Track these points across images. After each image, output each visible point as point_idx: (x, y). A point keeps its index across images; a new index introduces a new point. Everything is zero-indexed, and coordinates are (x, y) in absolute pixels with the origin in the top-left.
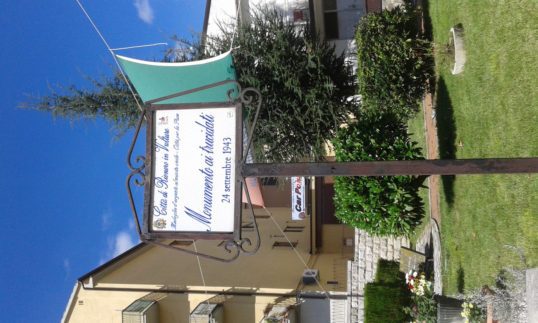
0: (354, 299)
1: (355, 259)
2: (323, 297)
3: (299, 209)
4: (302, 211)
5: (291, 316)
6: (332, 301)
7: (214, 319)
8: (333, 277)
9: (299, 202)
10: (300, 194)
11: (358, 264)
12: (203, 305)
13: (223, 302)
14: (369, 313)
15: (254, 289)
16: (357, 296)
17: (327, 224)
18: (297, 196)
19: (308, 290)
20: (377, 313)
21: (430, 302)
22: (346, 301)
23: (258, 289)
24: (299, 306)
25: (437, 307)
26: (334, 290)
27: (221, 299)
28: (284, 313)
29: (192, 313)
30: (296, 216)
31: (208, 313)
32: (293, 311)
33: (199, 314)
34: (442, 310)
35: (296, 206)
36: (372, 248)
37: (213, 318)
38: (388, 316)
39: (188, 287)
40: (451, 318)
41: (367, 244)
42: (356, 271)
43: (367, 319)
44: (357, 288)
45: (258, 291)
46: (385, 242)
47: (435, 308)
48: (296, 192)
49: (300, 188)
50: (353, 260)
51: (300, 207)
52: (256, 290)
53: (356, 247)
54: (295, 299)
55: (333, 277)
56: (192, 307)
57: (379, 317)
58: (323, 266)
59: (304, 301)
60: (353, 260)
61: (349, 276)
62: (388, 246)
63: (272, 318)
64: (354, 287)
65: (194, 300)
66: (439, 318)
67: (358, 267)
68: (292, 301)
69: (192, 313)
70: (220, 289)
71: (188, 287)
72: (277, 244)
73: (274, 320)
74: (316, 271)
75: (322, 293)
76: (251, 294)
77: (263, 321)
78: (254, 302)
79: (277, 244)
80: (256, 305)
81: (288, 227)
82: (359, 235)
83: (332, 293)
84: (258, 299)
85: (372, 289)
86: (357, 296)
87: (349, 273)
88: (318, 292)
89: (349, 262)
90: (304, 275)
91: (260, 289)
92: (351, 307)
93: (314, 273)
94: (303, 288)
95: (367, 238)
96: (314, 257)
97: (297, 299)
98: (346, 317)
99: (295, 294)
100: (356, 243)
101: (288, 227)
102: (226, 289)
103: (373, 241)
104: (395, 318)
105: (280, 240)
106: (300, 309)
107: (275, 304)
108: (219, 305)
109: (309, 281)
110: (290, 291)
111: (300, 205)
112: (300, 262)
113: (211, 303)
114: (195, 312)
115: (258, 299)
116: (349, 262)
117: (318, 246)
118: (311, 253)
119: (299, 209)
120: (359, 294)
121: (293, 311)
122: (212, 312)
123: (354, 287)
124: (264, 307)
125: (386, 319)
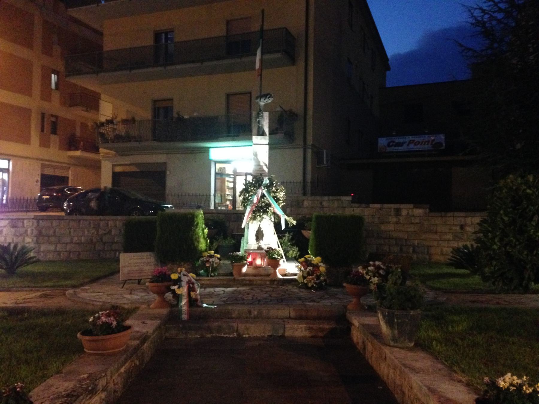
1: (353, 205)
3: (391, 144)
10: (408, 145)
18: (405, 142)
35: (394, 142)
50: (353, 202)
60: (353, 202)
111: (395, 146)
116: (349, 198)
119: (391, 144)
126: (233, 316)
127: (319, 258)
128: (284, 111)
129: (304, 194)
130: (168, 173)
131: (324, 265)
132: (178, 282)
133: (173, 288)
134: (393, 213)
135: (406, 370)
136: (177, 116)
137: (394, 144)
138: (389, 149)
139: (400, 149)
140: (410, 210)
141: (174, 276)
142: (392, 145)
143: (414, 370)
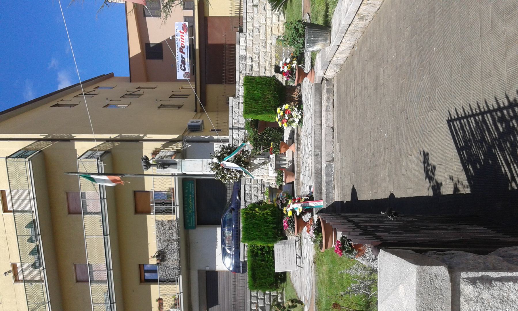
0: (236, 132)
4: (187, 71)
6: (215, 144)
7: (102, 163)
9: (183, 62)
10: (184, 53)
11: (239, 99)
13: (111, 149)
14: (247, 100)
15: (141, 135)
16: (238, 128)
17: (211, 83)
18: (182, 55)
19: (194, 136)
20: (254, 100)
23: (145, 135)
25: (305, 29)
27: (108, 146)
29: (79, 158)
33: (87, 158)
35: (181, 65)
37: (101, 161)
38: (264, 102)
39: (73, 135)
44: (238, 121)
45: (145, 138)
48: (180, 51)
49: (184, 47)
50: (234, 96)
52: (144, 136)
54: (181, 143)
56: (79, 154)
59: (189, 146)
60: (234, 96)
61: (231, 111)
65: (81, 147)
66: (307, 38)
67: (239, 103)
69: (79, 158)
71: (73, 135)
74: (201, 120)
75: (206, 138)
76: (139, 141)
78: (142, 148)
80: (143, 150)
82: (240, 72)
83: (215, 137)
85: (251, 79)
86: (238, 128)
87: (230, 108)
89: (231, 98)
90: (190, 123)
91: (147, 135)
93: (199, 122)
96: (199, 114)
97: (183, 144)
99: (181, 139)
101: (173, 95)
102: (113, 136)
104: (270, 103)
105: (164, 103)
108: (106, 152)
109: (194, 128)
110: (176, 136)
111: (185, 64)
113: (99, 150)
114: (83, 157)
115: (145, 144)
117: (203, 104)
118: (196, 111)
122: (100, 156)
127: (278, 110)
130: (207, 269)
132: (294, 211)
133: (298, 214)
134: (243, 62)
136: (155, 259)
137: (183, 65)
138: (188, 70)
139: (187, 60)
140: (241, 47)
141: (290, 214)
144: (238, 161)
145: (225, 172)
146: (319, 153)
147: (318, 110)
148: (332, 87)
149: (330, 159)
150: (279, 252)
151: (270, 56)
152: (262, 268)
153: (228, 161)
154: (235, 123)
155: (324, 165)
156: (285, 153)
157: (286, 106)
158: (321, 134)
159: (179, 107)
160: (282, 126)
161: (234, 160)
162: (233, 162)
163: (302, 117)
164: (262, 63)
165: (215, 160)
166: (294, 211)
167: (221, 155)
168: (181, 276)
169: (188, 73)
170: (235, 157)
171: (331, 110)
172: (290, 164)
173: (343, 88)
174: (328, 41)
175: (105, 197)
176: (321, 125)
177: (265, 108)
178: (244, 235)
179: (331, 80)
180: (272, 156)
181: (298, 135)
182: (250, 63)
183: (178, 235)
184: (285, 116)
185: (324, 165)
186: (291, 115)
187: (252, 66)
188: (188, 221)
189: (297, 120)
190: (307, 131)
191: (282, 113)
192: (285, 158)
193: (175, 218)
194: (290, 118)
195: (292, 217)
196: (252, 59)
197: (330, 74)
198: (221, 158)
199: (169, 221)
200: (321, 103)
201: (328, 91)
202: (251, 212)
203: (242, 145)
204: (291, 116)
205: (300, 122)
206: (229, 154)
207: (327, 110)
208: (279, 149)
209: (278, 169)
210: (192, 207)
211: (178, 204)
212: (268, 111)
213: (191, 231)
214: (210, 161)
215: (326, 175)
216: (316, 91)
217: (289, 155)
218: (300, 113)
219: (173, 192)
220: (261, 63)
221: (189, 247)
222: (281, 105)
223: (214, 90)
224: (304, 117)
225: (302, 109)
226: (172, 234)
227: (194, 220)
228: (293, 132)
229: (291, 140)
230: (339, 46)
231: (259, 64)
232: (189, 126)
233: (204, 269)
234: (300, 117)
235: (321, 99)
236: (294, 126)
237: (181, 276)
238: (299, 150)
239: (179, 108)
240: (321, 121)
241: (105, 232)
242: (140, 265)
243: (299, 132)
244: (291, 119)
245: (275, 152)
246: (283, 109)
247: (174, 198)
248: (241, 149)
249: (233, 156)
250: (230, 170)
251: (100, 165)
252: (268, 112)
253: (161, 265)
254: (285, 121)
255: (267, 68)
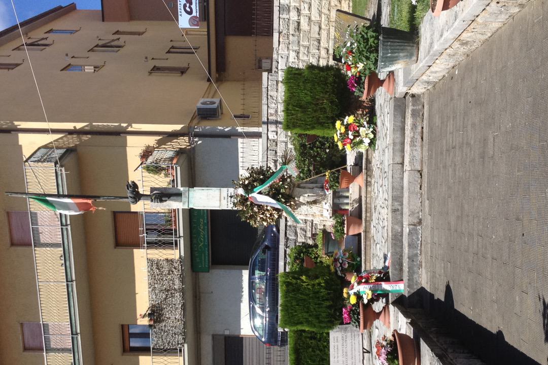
0: (272, 128)
1: (274, 69)
2: (227, 136)
3: (188, 9)
4: (194, 14)
5: (181, 161)
6: (240, 140)
7: (63, 169)
8: (242, 107)
11: (277, 76)
12: (43, 151)
13: (76, 146)
14: (290, 107)
15: (124, 125)
16: (276, 123)
19: (207, 126)
20: (301, 107)
21: (369, 35)
22: (261, 140)
23: (130, 125)
24: (194, 148)
25: (378, 39)
26: (244, 125)
27: (73, 141)
28: (171, 159)
29: (27, 161)
30: (184, 21)
31: (54, 160)
32: (183, 158)
33: (39, 161)
34: (386, 44)
35: (185, 6)
36: (298, 53)
37: (61, 166)
38: (315, 111)
39: (16, 123)
40: (397, 54)
41: (290, 48)
42: (275, 87)
43: (288, 116)
44: (276, 111)
45: (130, 129)
46: (316, 43)
47: (376, 42)
51: (190, 7)
52: (127, 127)
53: (275, 52)
54: (186, 138)
55: (242, 107)
56: (27, 153)
57: (302, 112)
58: (227, 97)
59: (199, 143)
61: (264, 95)
62: (321, 49)
63: (153, 164)
64: (271, 111)
65: (29, 143)
66: (381, 54)
67: (277, 82)
68: (183, 143)
69: (27, 161)
70: (69, 126)
71: (16, 123)
72: (156, 69)
73: (157, 167)
74: (217, 101)
75: (226, 130)
76: (120, 133)
77: (140, 169)
78: (124, 145)
79: (156, 69)
81: (173, 47)
82: (280, 33)
83: (240, 129)
84: (130, 139)
85: (295, 74)
86: (276, 123)
87: (264, 90)
88: (220, 128)
89: (265, 75)
90: (199, 105)
91: (134, 125)
92: (268, 138)
93: (214, 103)
94: (198, 123)
95: (291, 37)
97: (190, 139)
98: (261, 156)
99: (187, 132)
100: (275, 44)
102: (79, 126)
103: (299, 42)
104: (325, 112)
106: (194, 153)
107: (157, 148)
108: (70, 151)
109: (207, 114)
110: (178, 127)
112: (194, 92)
113: (58, 148)
114: (32, 159)
115: (130, 139)
117: (220, 69)
119: (189, 10)
120: (279, 120)
121: (183, 158)
122: (60, 158)
123: (271, 111)
124: (140, 151)
125: (314, 114)
126: (399, 230)
128: (141, 164)
129: (258, 135)
130: (227, 333)
131: (347, 117)
133: (366, 301)
134: (284, 16)
135: (431, 52)
136: (147, 319)
137: (188, 5)
141: (353, 300)
142: (190, 7)
143: (431, 44)
144: (274, 193)
145: (255, 209)
146: (399, 208)
147: (398, 141)
148: (420, 107)
149: (416, 221)
150: (336, 344)
151: (327, 6)
152: (310, 350)
153: (260, 193)
154: (272, 115)
155: (406, 230)
156: (348, 188)
157: (350, 119)
158: (402, 179)
159: (183, 71)
160: (344, 149)
161: (269, 192)
162: (268, 195)
163: (375, 136)
164: (315, 16)
165: (241, 191)
166: (359, 296)
167: (249, 183)
168: (186, 346)
169: (196, 17)
170: (271, 187)
171: (418, 144)
172: (356, 205)
173: (437, 120)
174: (414, 58)
175: (69, 223)
176: (402, 164)
177: (318, 119)
178: (283, 316)
179: (419, 96)
180: (329, 193)
181: (368, 162)
182: (296, 18)
183: (182, 282)
184: (348, 134)
185: (406, 230)
186: (358, 132)
187: (299, 23)
188: (198, 260)
189: (367, 141)
190: (382, 158)
191: (343, 130)
192: (347, 194)
193: (177, 257)
194: (355, 137)
195: (357, 304)
196: (298, 10)
197: (416, 90)
198: (249, 188)
199: (167, 260)
200: (403, 129)
201: (415, 114)
202: (294, 281)
203: (281, 169)
204: (357, 134)
205: (372, 143)
206: (262, 182)
207: (413, 144)
208: (338, 183)
209: (337, 211)
210: (204, 238)
211: (182, 234)
212: (322, 125)
213: (201, 275)
214: (231, 190)
215: (409, 245)
216: (395, 110)
217: (354, 190)
218: (371, 129)
219: (175, 217)
220: (313, 18)
221: (199, 299)
222: (341, 116)
223: (238, 46)
224: (377, 137)
225: (375, 124)
226: (173, 280)
227: (205, 257)
228: (359, 157)
229: (357, 168)
230: (430, 66)
231: (310, 18)
232: (199, 109)
233: (221, 333)
234: (372, 136)
235: (404, 123)
236: (362, 149)
237: (186, 346)
238: (370, 186)
239: (182, 73)
240: (403, 157)
241: (74, 330)
242: (122, 326)
243: (370, 157)
244: (358, 139)
245: (331, 187)
246: (345, 123)
247: (175, 225)
248: (281, 175)
249: (268, 185)
250: (263, 207)
251: (59, 173)
252: (322, 126)
253: (155, 328)
254: (349, 141)
255: (323, 26)
